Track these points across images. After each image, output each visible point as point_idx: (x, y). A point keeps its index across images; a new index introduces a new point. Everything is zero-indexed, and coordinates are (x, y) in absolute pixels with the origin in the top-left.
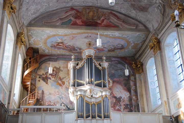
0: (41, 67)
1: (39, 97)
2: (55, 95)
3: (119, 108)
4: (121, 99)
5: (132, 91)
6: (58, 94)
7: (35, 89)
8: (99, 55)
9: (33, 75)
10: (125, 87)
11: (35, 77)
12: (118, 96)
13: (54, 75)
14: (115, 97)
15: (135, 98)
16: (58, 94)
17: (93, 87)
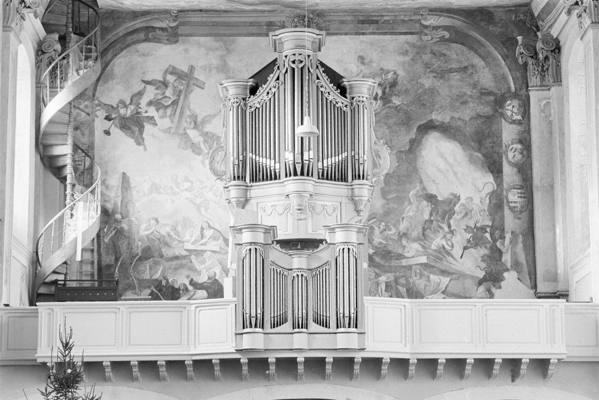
0: (112, 70)
1: (112, 202)
2: (174, 194)
3: (444, 243)
4: (457, 206)
5: (508, 171)
6: (186, 190)
7: (91, 168)
8: (366, 6)
9: (81, 107)
10: (479, 150)
11: (88, 114)
12: (442, 194)
13: (168, 106)
14: (431, 198)
15: (519, 200)
16: (186, 190)
17: (310, 184)
